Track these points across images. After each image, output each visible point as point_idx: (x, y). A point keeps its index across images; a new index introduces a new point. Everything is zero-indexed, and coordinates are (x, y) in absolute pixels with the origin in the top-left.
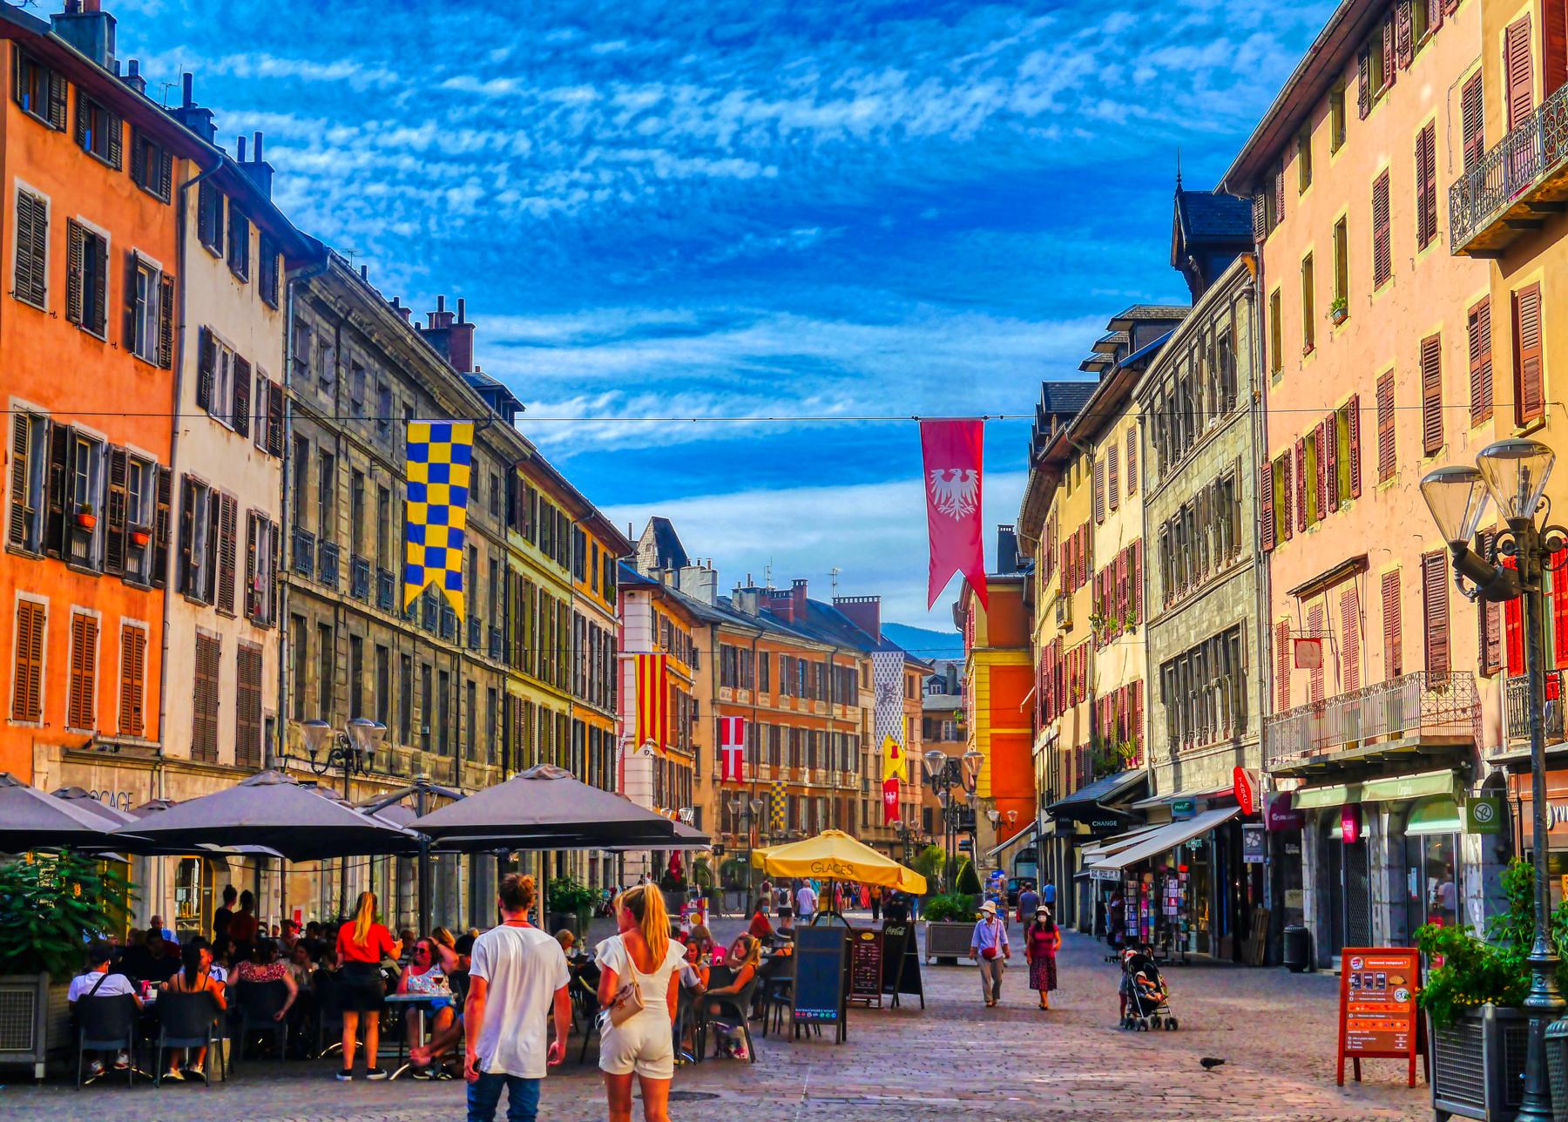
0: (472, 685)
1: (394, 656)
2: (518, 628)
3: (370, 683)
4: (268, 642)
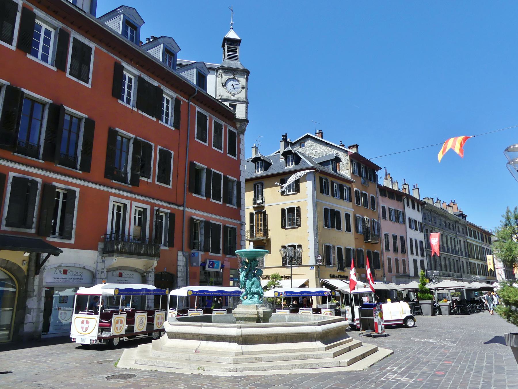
0: (463, 262)
1: (447, 259)
2: (469, 251)
3: (443, 263)
4: (425, 259)
